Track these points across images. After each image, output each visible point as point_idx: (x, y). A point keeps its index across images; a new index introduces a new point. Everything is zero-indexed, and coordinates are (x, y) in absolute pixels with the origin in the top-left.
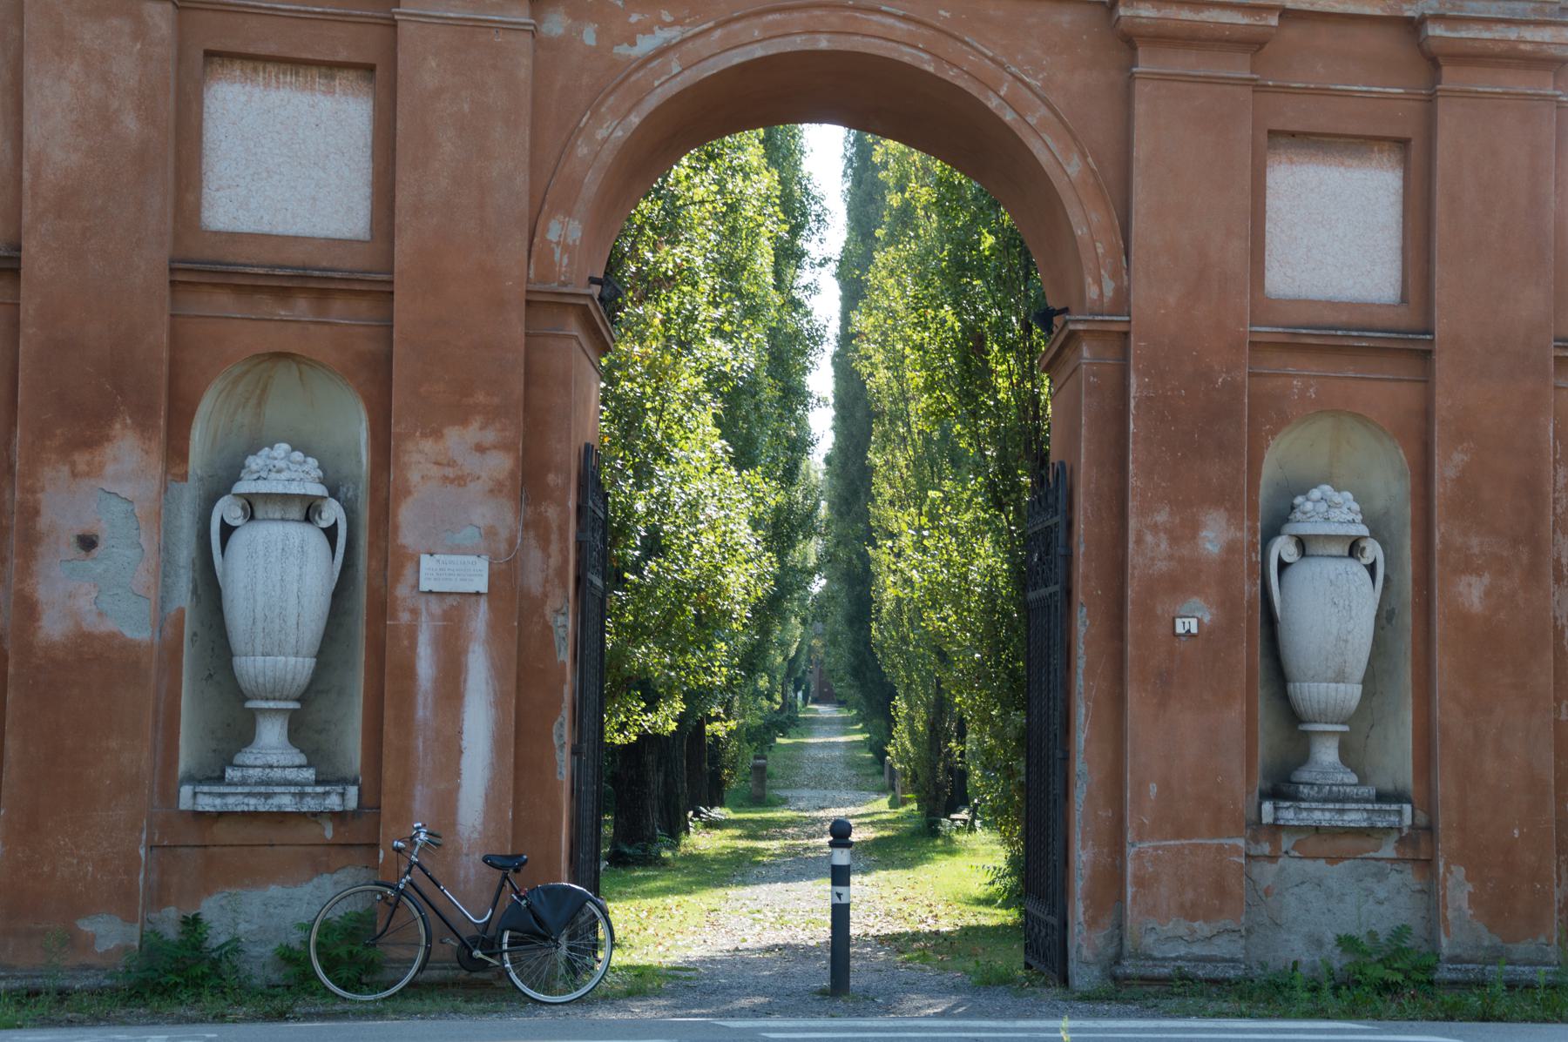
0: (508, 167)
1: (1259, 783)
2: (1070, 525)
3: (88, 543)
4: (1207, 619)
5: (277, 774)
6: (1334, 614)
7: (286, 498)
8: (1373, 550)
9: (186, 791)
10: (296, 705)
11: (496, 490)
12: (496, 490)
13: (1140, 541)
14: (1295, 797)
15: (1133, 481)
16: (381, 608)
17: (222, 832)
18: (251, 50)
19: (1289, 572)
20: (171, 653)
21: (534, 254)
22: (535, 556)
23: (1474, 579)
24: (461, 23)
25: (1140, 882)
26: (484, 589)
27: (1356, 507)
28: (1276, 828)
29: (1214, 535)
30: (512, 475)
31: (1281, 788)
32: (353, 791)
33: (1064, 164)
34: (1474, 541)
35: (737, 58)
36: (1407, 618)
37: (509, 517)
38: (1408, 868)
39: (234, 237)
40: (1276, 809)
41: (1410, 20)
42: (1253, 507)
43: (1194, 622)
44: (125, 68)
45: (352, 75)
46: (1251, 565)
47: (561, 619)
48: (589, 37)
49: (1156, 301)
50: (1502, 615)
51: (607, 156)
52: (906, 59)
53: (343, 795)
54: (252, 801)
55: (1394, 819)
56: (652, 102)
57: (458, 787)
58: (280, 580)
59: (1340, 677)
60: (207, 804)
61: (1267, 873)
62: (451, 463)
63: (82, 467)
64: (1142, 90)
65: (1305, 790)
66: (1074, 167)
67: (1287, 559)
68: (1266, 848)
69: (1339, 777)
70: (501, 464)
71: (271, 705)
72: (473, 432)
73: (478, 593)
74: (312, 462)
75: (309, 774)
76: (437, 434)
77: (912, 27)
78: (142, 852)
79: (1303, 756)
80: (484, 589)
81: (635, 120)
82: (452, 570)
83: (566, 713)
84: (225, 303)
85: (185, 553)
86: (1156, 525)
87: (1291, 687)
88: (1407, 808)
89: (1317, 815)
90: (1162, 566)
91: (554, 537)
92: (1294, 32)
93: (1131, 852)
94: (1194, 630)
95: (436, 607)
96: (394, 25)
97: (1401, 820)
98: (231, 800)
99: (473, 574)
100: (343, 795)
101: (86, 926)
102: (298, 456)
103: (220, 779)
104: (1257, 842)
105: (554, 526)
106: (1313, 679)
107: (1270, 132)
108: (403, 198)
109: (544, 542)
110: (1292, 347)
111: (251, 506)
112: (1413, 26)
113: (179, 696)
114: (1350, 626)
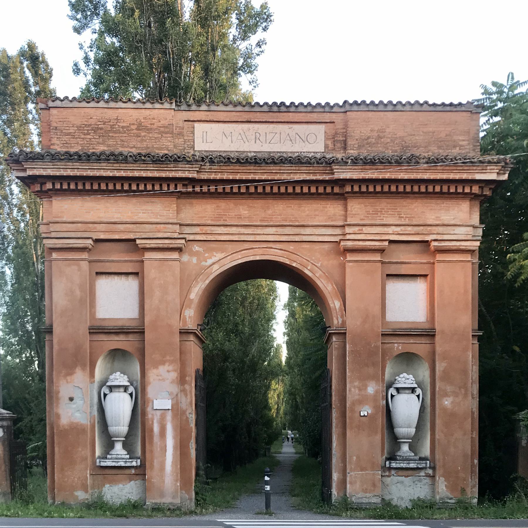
0: (174, 295)
1: (386, 455)
2: (331, 386)
3: (71, 399)
4: (370, 412)
5: (120, 456)
6: (407, 409)
7: (119, 387)
8: (419, 391)
11: (172, 382)
14: (395, 459)
15: (348, 374)
16: (144, 414)
17: (108, 471)
18: (107, 271)
19: (394, 398)
21: (181, 318)
22: (184, 399)
23: (448, 398)
25: (351, 483)
26: (170, 407)
27: (414, 379)
28: (390, 468)
29: (371, 390)
30: (177, 378)
31: (392, 458)
32: (139, 461)
33: (326, 287)
36: (428, 410)
38: (428, 478)
39: (104, 319)
40: (390, 463)
42: (383, 380)
45: (133, 276)
46: (383, 396)
47: (191, 415)
49: (353, 323)
50: (456, 409)
53: (136, 462)
54: (114, 463)
55: (424, 465)
57: (166, 459)
58: (120, 407)
59: (409, 427)
60: (103, 464)
61: (388, 480)
62: (161, 376)
63: (69, 380)
64: (348, 265)
67: (393, 394)
68: (387, 474)
69: (408, 454)
70: (174, 375)
72: (167, 367)
73: (169, 409)
74: (126, 377)
75: (128, 456)
78: (88, 476)
79: (399, 449)
83: (193, 440)
86: (355, 386)
87: (395, 429)
88: (428, 462)
89: (402, 465)
90: (357, 397)
92: (393, 246)
94: (366, 415)
95: (159, 413)
96: (143, 261)
97: (426, 465)
100: (136, 462)
101: (76, 493)
102: (122, 375)
103: (106, 458)
104: (385, 472)
105: (188, 391)
106: (401, 427)
110: (394, 335)
113: (95, 437)
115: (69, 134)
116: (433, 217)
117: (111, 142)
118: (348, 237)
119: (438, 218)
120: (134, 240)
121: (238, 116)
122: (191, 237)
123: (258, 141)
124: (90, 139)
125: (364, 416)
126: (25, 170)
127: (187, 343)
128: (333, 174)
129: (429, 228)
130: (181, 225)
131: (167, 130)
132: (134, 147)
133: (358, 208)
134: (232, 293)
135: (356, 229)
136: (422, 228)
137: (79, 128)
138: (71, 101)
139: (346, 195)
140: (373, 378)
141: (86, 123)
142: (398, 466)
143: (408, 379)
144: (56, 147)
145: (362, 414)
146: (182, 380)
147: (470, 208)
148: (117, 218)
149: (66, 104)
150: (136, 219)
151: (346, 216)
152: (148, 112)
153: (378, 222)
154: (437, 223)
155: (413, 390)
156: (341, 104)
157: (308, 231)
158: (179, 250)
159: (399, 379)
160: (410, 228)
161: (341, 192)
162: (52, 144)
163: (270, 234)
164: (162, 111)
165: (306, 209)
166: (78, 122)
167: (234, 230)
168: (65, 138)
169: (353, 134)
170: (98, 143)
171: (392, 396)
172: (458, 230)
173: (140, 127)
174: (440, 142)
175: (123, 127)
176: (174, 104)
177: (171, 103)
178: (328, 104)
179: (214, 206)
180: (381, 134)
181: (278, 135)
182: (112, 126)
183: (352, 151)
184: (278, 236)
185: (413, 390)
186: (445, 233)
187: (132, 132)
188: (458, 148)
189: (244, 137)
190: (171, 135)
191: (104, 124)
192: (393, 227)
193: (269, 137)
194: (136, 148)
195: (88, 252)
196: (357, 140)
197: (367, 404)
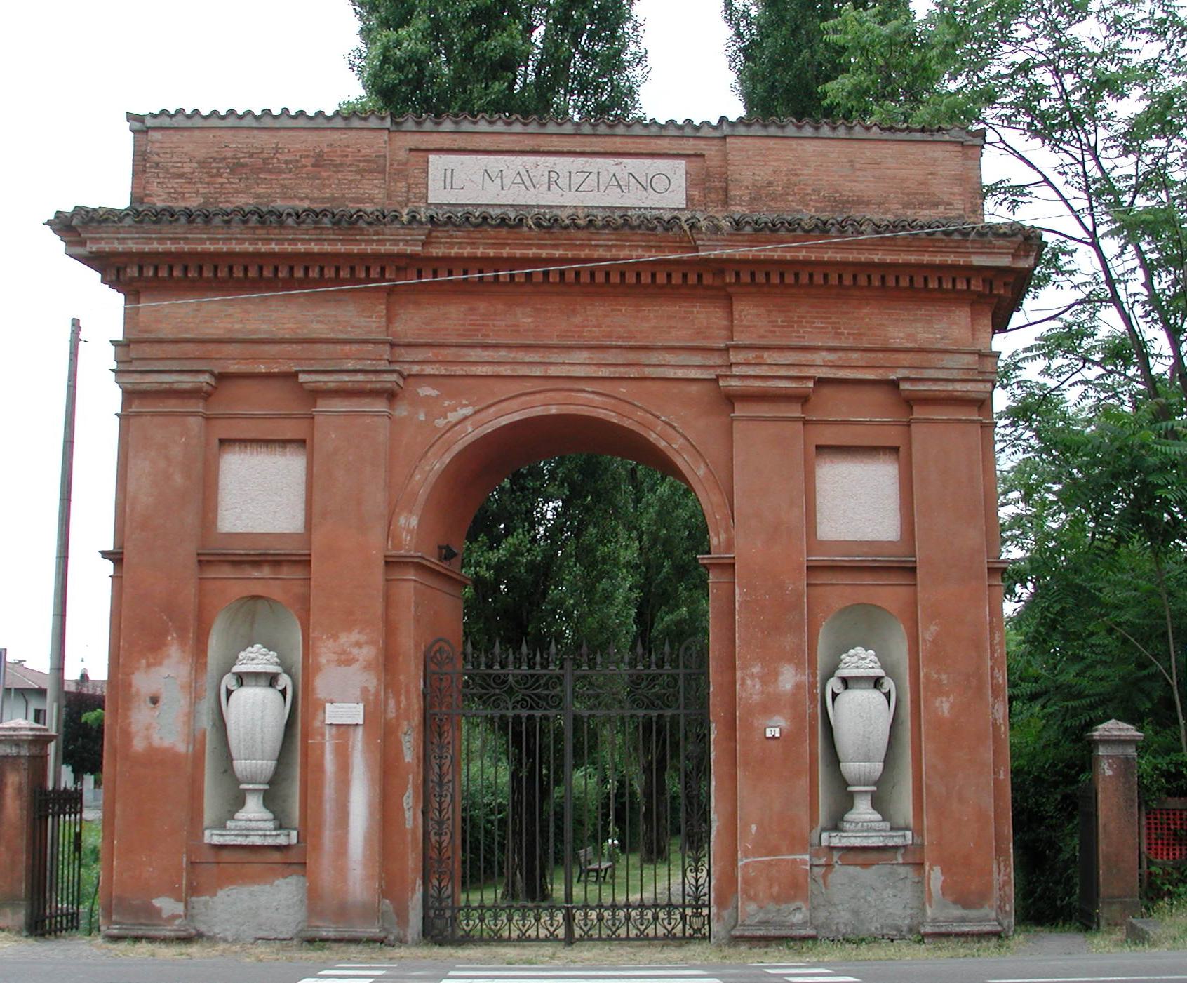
3: (155, 700)
5: (253, 824)
7: (256, 675)
9: (207, 833)
10: (267, 787)
12: (367, 667)
13: (743, 684)
17: (225, 856)
18: (242, 436)
20: (198, 759)
24: (347, 414)
26: (361, 722)
27: (876, 659)
29: (788, 679)
32: (294, 834)
34: (944, 677)
35: (504, 421)
37: (375, 682)
38: (908, 868)
41: (893, 381)
43: (778, 730)
44: (176, 452)
45: (294, 445)
48: (422, 417)
51: (432, 478)
52: (601, 416)
56: (457, 448)
60: (217, 840)
62: (344, 652)
65: (847, 826)
66: (701, 472)
71: (251, 786)
72: (355, 636)
76: (335, 637)
77: (605, 399)
80: (361, 722)
81: (447, 459)
82: (345, 711)
84: (227, 572)
85: (206, 706)
90: (756, 698)
91: (403, 692)
92: (827, 391)
93: (740, 864)
94: (777, 735)
98: (228, 838)
99: (352, 713)
101: (157, 902)
103: (224, 827)
106: (852, 761)
107: (817, 447)
108: (317, 509)
109: (397, 696)
111: (241, 679)
112: (895, 384)
114: (871, 729)
115: (180, 176)
116: (901, 335)
117: (260, 190)
118: (736, 371)
119: (910, 337)
120: (295, 375)
121: (513, 141)
122: (415, 369)
123: (553, 187)
124: (222, 184)
125: (774, 737)
126: (83, 243)
127: (401, 584)
128: (696, 249)
129: (896, 356)
130: (393, 345)
131: (374, 166)
132: (307, 198)
133: (753, 318)
134: (497, 479)
135: (751, 356)
136: (880, 355)
137: (203, 164)
138: (188, 117)
139: (729, 289)
140: (793, 657)
141: (215, 155)
142: (845, 843)
143: (864, 659)
144: (155, 200)
145: (769, 734)
146: (388, 663)
147: (973, 320)
148: (265, 332)
149: (198, 122)
150: (304, 333)
151: (731, 329)
152: (336, 135)
153: (795, 342)
154: (910, 345)
155: (877, 683)
156: (715, 123)
157: (655, 358)
158: (391, 395)
159: (847, 659)
160: (856, 355)
161: (718, 282)
162: (147, 195)
163: (578, 364)
164: (365, 133)
165: (652, 315)
166: (201, 154)
167: (503, 354)
168: (175, 183)
169: (738, 176)
170: (237, 192)
171: (835, 695)
172: (949, 360)
173: (320, 161)
174: (908, 194)
175: (286, 162)
176: (389, 119)
177: (383, 119)
178: (689, 122)
179: (464, 307)
180: (794, 179)
181: (594, 176)
182: (265, 161)
183: (738, 208)
184: (594, 368)
185: (877, 683)
186: (925, 364)
187: (305, 170)
188: (941, 208)
189: (526, 178)
190: (381, 176)
191: (251, 156)
192: (824, 354)
193: (576, 180)
194: (311, 200)
195: (202, 398)
196: (747, 188)
197: (778, 712)
